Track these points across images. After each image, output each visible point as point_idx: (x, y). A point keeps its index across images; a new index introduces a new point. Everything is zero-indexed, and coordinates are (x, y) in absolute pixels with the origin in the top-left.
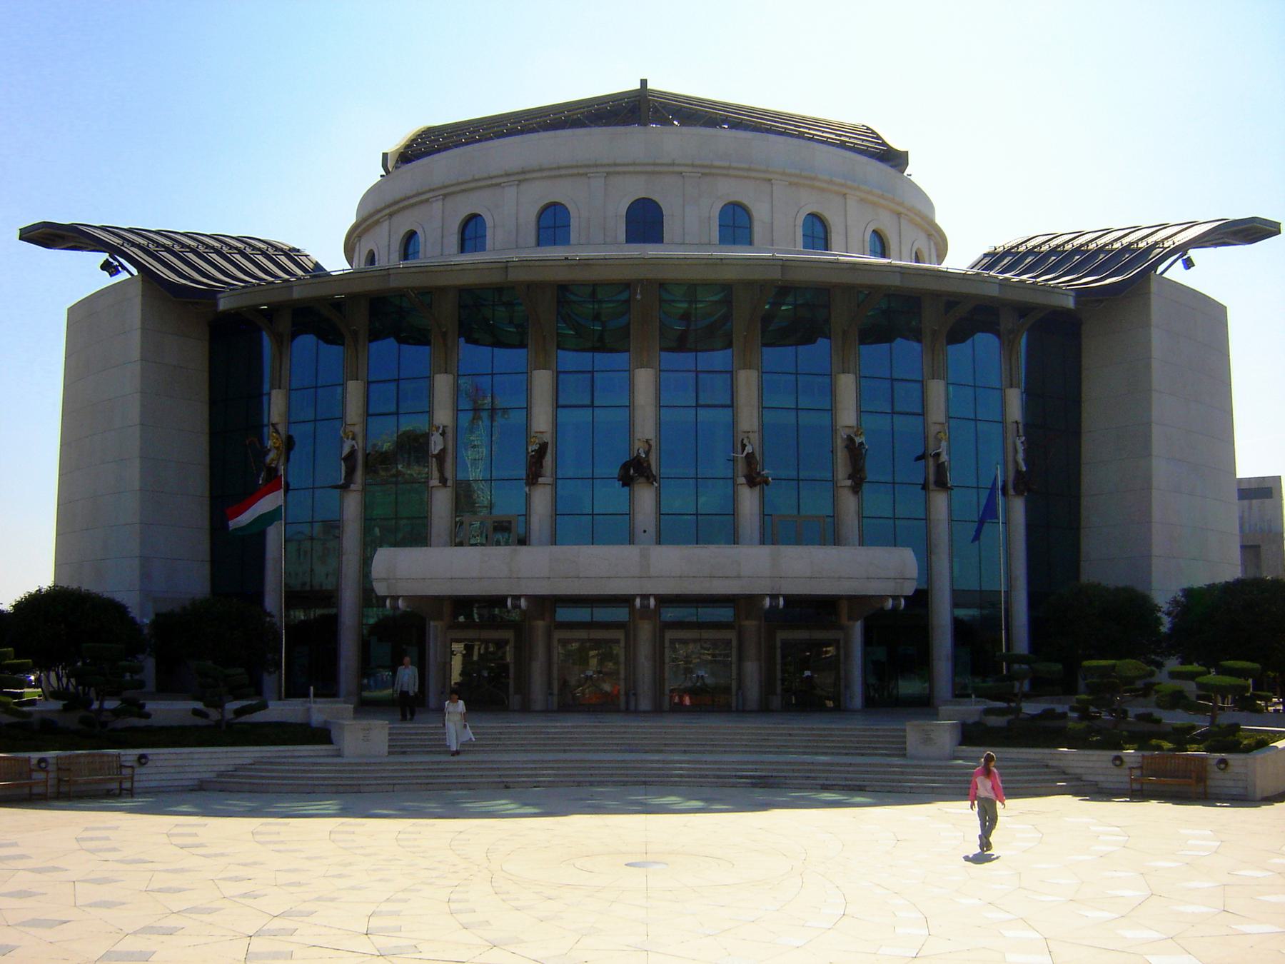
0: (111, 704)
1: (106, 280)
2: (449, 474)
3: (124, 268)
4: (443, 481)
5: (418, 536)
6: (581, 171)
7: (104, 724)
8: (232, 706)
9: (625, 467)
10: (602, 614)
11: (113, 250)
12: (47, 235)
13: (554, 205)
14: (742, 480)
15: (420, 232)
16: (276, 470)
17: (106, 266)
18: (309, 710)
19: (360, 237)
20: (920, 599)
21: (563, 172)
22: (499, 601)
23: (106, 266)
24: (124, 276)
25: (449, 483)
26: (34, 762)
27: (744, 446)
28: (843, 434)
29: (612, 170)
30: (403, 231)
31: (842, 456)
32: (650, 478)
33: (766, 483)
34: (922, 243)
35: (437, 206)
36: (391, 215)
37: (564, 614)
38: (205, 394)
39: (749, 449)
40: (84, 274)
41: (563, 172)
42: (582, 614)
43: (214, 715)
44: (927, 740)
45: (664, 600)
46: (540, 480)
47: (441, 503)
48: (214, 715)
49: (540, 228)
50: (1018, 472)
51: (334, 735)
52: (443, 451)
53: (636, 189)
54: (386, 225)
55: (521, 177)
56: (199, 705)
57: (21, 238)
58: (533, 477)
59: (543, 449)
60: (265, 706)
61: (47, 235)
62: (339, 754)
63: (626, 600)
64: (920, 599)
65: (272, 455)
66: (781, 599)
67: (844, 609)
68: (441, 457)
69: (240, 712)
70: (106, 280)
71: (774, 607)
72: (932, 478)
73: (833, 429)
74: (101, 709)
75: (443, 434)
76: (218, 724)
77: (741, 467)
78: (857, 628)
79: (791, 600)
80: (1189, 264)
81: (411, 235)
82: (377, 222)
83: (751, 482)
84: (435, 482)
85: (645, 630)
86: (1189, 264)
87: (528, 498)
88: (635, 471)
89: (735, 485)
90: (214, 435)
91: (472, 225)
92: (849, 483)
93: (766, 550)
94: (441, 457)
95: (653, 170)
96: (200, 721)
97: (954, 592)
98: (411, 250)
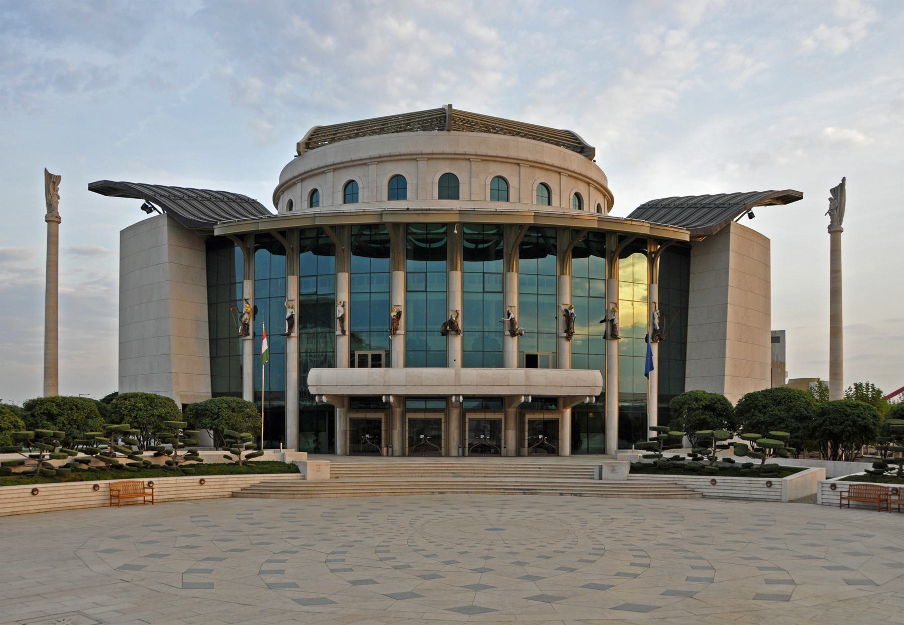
0: (182, 453)
1: (144, 216)
2: (347, 328)
3: (155, 209)
4: (343, 332)
5: (329, 362)
6: (413, 157)
7: (177, 463)
8: (245, 453)
9: (445, 325)
10: (431, 405)
11: (148, 198)
12: (105, 188)
14: (508, 333)
15: (320, 190)
16: (248, 325)
17: (144, 208)
18: (283, 455)
19: (283, 192)
20: (602, 398)
21: (403, 157)
23: (144, 208)
24: (154, 214)
25: (347, 333)
26: (146, 483)
27: (509, 315)
28: (563, 308)
29: (432, 157)
31: (562, 319)
32: (457, 332)
33: (521, 334)
34: (601, 200)
35: (330, 175)
36: (302, 180)
37: (410, 404)
39: (512, 316)
40: (132, 211)
41: (403, 157)
42: (421, 405)
43: (235, 458)
44: (613, 470)
46: (398, 332)
47: (343, 345)
48: (235, 458)
49: (390, 189)
50: (655, 330)
51: (300, 468)
52: (344, 315)
54: (299, 185)
55: (380, 160)
56: (228, 453)
57: (90, 189)
58: (393, 331)
59: (399, 314)
60: (262, 454)
61: (105, 188)
62: (304, 478)
63: (445, 398)
64: (602, 398)
65: (246, 316)
66: (530, 398)
67: (561, 402)
68: (342, 319)
69: (248, 457)
70: (144, 216)
72: (609, 333)
73: (558, 307)
74: (176, 455)
75: (343, 306)
76: (237, 463)
78: (568, 413)
79: (536, 398)
80: (751, 216)
81: (315, 191)
82: (294, 184)
83: (513, 334)
84: (339, 332)
85: (455, 414)
86: (751, 216)
87: (390, 341)
88: (449, 328)
89: (503, 336)
90: (210, 305)
91: (350, 186)
92: (565, 335)
93: (523, 371)
94: (342, 319)
95: (454, 157)
96: (227, 461)
97: (620, 394)
98: (314, 200)
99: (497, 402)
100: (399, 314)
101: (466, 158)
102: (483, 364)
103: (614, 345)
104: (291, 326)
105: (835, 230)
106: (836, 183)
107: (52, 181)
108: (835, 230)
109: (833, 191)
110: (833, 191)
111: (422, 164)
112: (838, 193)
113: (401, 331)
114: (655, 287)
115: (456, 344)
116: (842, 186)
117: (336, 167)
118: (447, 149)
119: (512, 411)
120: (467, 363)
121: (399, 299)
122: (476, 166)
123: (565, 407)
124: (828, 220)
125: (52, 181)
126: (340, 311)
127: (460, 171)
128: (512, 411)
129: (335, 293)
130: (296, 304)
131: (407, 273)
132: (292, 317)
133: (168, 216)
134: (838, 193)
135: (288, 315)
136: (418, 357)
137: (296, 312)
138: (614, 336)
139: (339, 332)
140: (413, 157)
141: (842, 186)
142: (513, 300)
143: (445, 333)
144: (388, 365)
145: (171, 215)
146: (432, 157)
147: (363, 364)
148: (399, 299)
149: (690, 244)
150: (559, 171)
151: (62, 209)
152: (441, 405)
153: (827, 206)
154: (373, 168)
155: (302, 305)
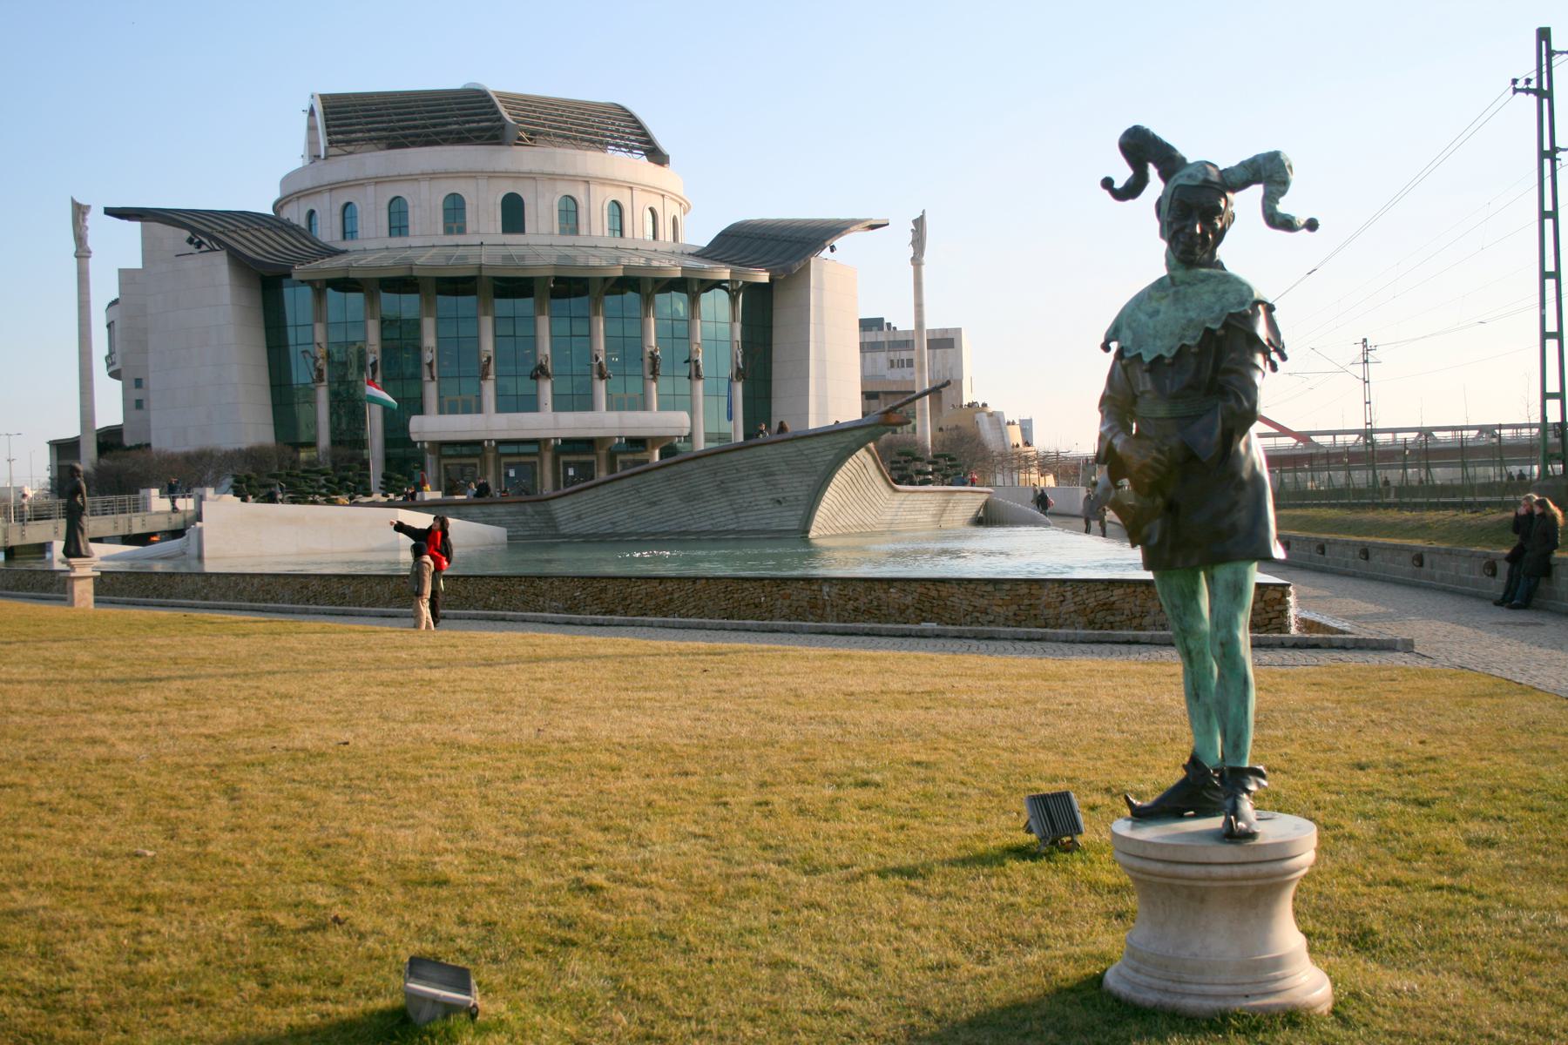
6: (472, 175)
13: (454, 194)
15: (357, 204)
17: (190, 241)
22: (479, 443)
23: (190, 241)
29: (493, 175)
30: (346, 200)
31: (648, 361)
37: (503, 449)
38: (262, 324)
42: (514, 449)
45: (500, 442)
53: (508, 187)
55: (433, 176)
58: (484, 376)
67: (649, 444)
68: (430, 365)
71: (556, 445)
73: (643, 349)
77: (595, 370)
83: (602, 377)
87: (480, 387)
88: (540, 372)
93: (614, 415)
94: (430, 365)
95: (518, 176)
97: (706, 434)
100: (489, 359)
101: (531, 176)
102: (572, 408)
103: (700, 385)
104: (374, 372)
105: (917, 261)
106: (918, 216)
107: (79, 211)
108: (917, 261)
109: (915, 222)
110: (915, 222)
111: (482, 182)
112: (919, 223)
113: (492, 376)
114: (738, 326)
115: (546, 388)
116: (922, 217)
117: (378, 181)
118: (512, 167)
119: (603, 453)
120: (557, 408)
121: (488, 344)
123: (653, 448)
124: (910, 252)
125: (79, 211)
126: (428, 357)
127: (525, 191)
128: (603, 453)
130: (377, 348)
131: (495, 319)
132: (375, 363)
133: (229, 254)
134: (919, 223)
135: (371, 360)
136: (507, 403)
137: (378, 357)
138: (698, 376)
139: (427, 377)
140: (472, 175)
141: (922, 217)
142: (600, 343)
143: (535, 377)
144: (479, 410)
146: (493, 175)
148: (488, 344)
149: (770, 264)
151: (91, 243)
152: (534, 448)
154: (424, 185)
155: (384, 350)
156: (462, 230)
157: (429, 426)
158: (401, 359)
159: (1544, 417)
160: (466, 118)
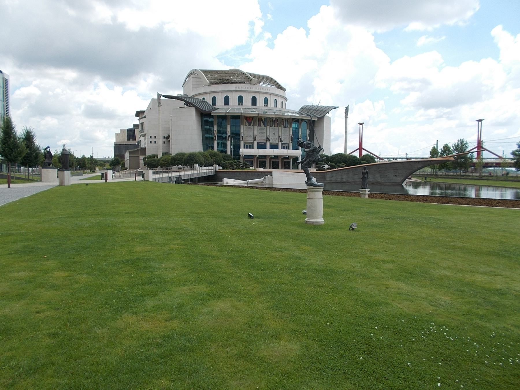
23: (185, 104)
29: (250, 92)
55: (236, 91)
95: (256, 92)
99: (265, 157)
105: (346, 117)
108: (346, 117)
111: (247, 93)
112: (347, 108)
117: (222, 92)
122: (261, 95)
124: (345, 114)
129: (240, 131)
134: (347, 108)
145: (197, 109)
146: (250, 92)
147: (247, 148)
150: (279, 96)
153: (344, 111)
154: (234, 93)
156: (242, 105)
157: (243, 151)
158: (236, 136)
159: (484, 159)
160: (237, 77)
